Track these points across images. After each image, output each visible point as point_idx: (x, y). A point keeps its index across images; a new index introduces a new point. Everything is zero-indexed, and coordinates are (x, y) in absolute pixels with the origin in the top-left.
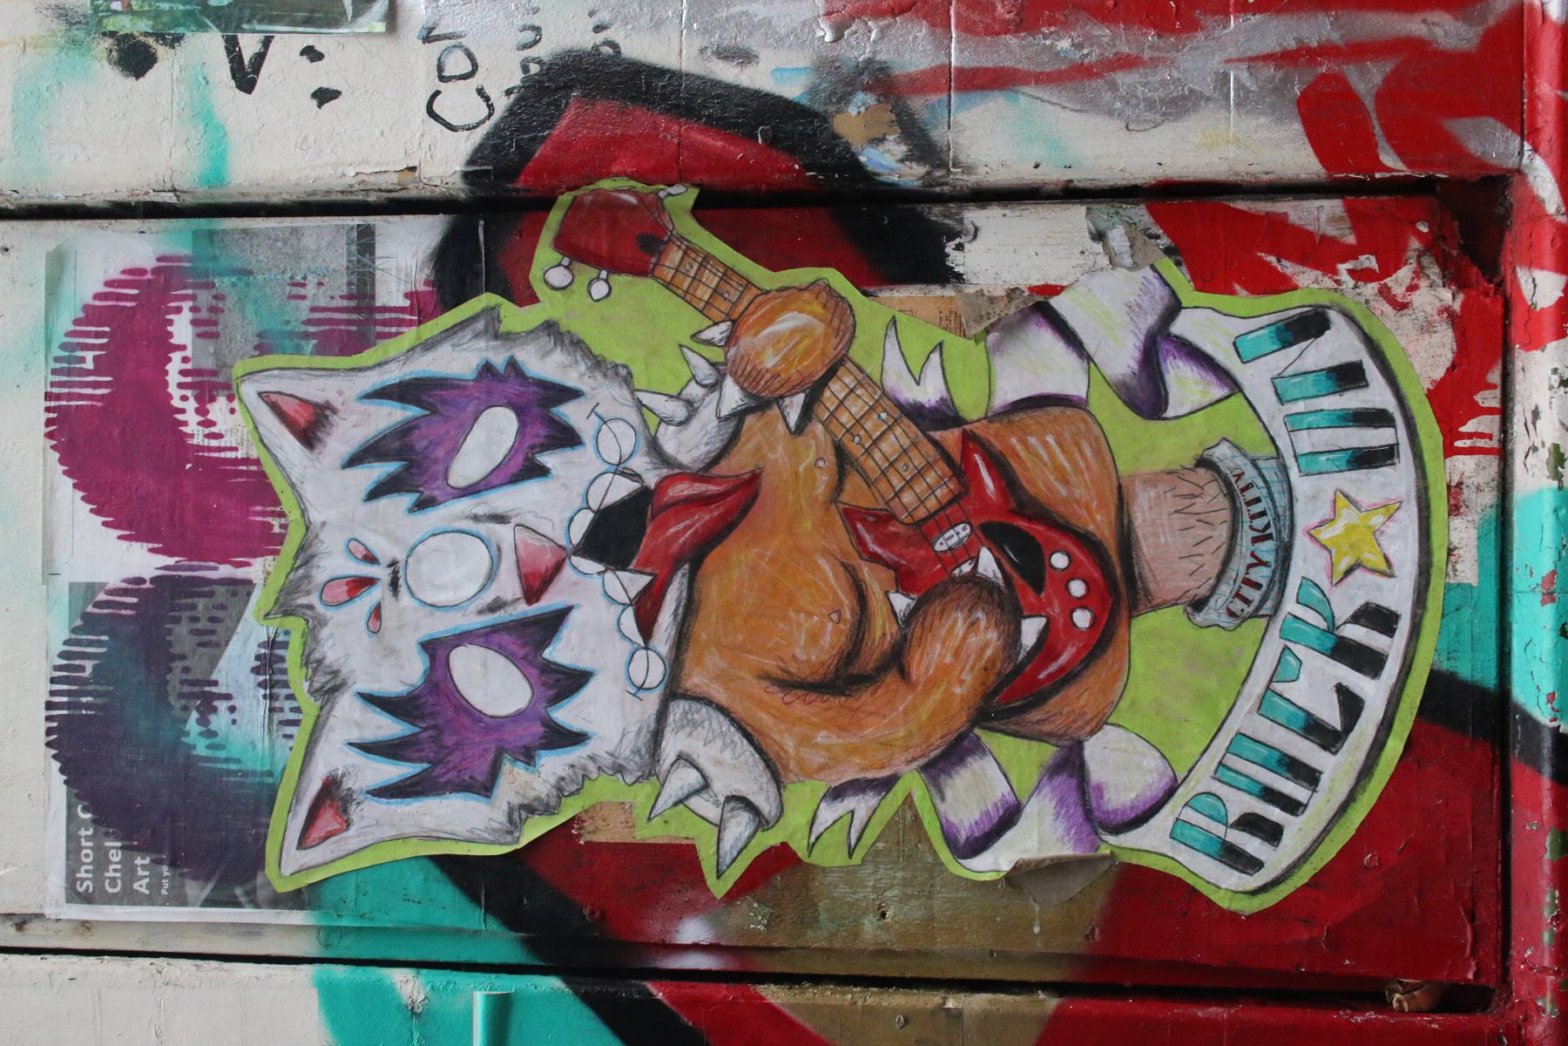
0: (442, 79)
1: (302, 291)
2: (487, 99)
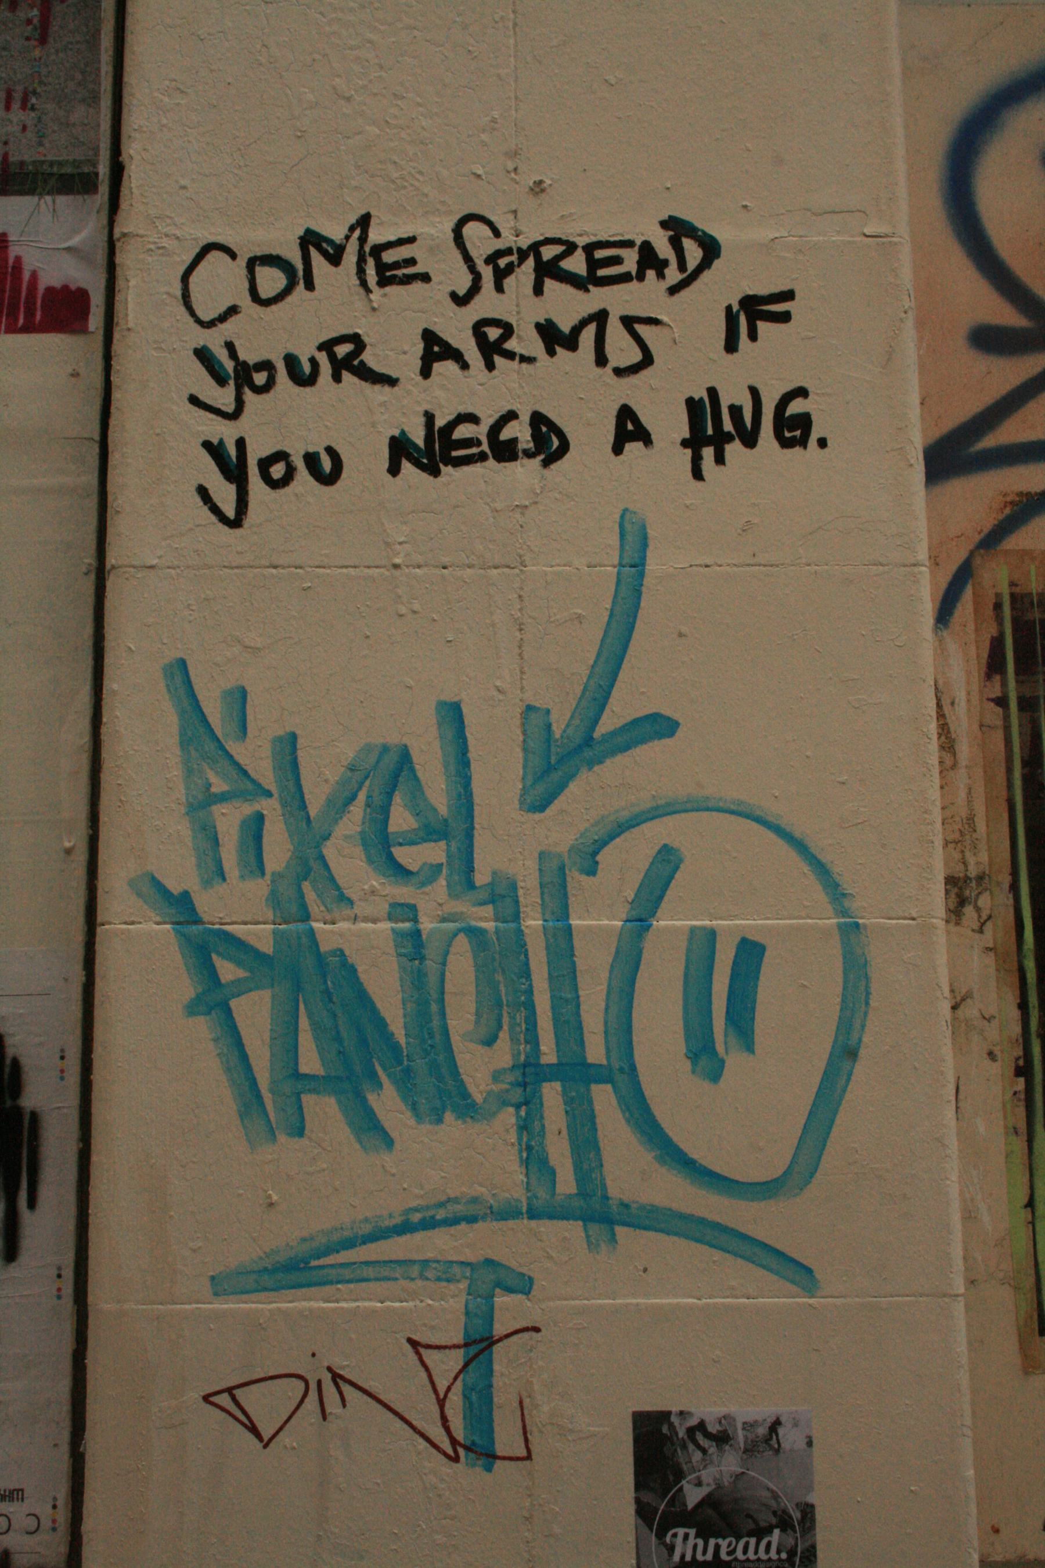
0: (252, 264)
1: (16, 106)
2: (223, 318)
